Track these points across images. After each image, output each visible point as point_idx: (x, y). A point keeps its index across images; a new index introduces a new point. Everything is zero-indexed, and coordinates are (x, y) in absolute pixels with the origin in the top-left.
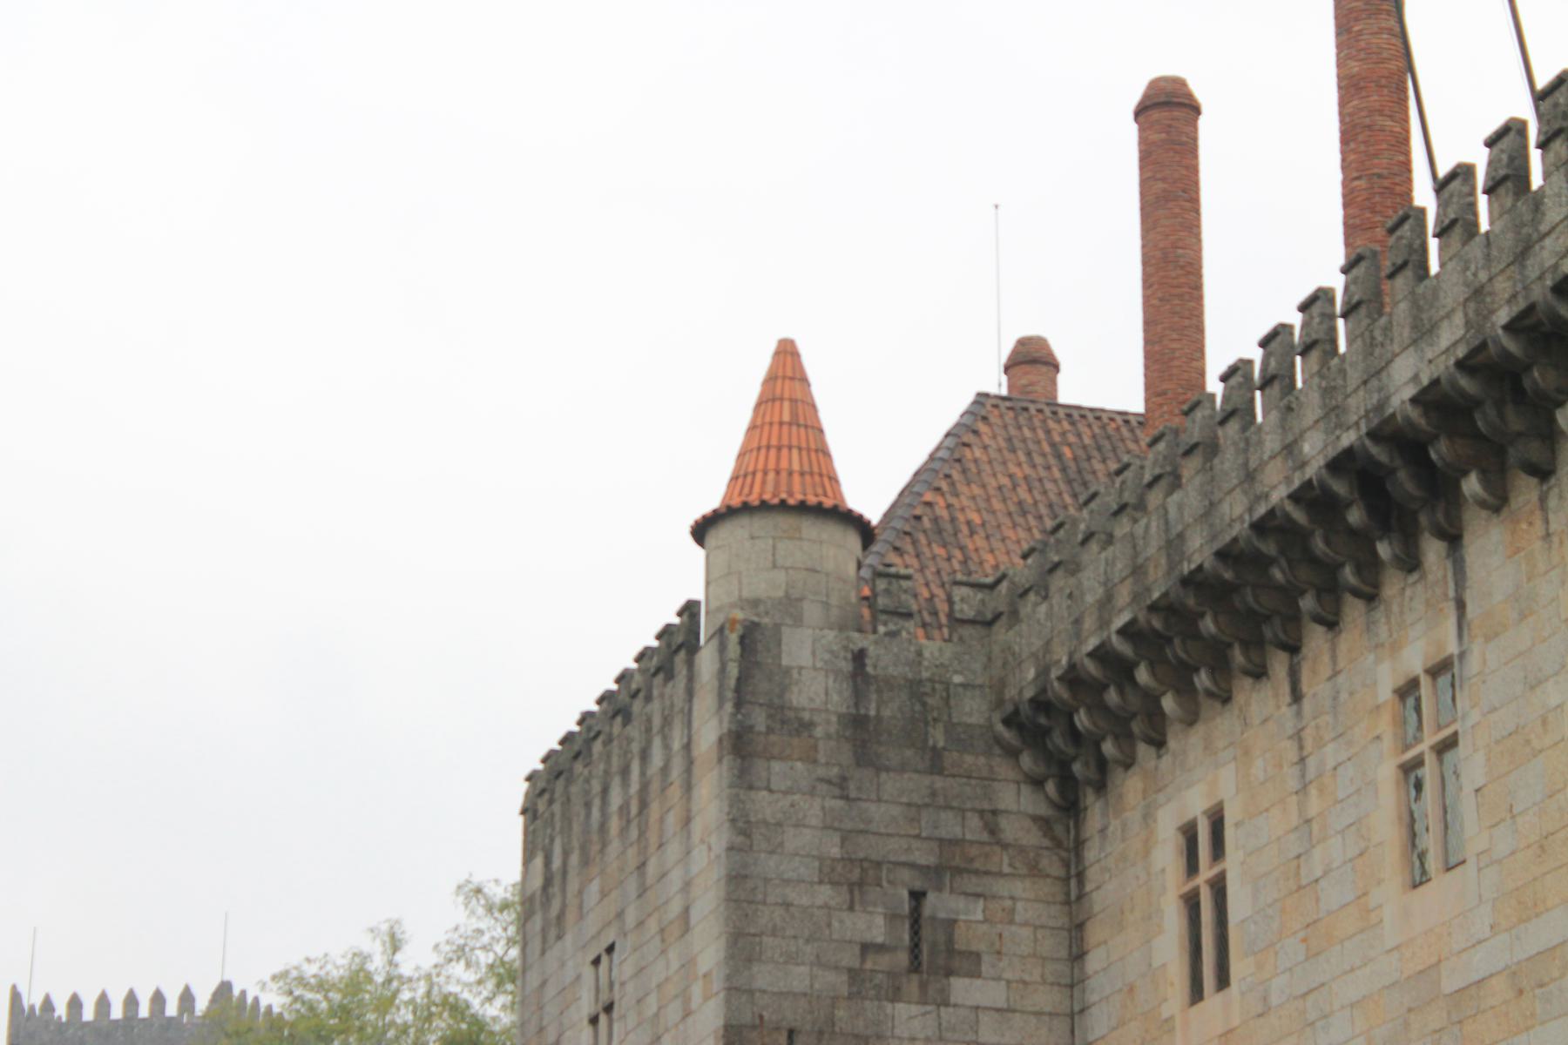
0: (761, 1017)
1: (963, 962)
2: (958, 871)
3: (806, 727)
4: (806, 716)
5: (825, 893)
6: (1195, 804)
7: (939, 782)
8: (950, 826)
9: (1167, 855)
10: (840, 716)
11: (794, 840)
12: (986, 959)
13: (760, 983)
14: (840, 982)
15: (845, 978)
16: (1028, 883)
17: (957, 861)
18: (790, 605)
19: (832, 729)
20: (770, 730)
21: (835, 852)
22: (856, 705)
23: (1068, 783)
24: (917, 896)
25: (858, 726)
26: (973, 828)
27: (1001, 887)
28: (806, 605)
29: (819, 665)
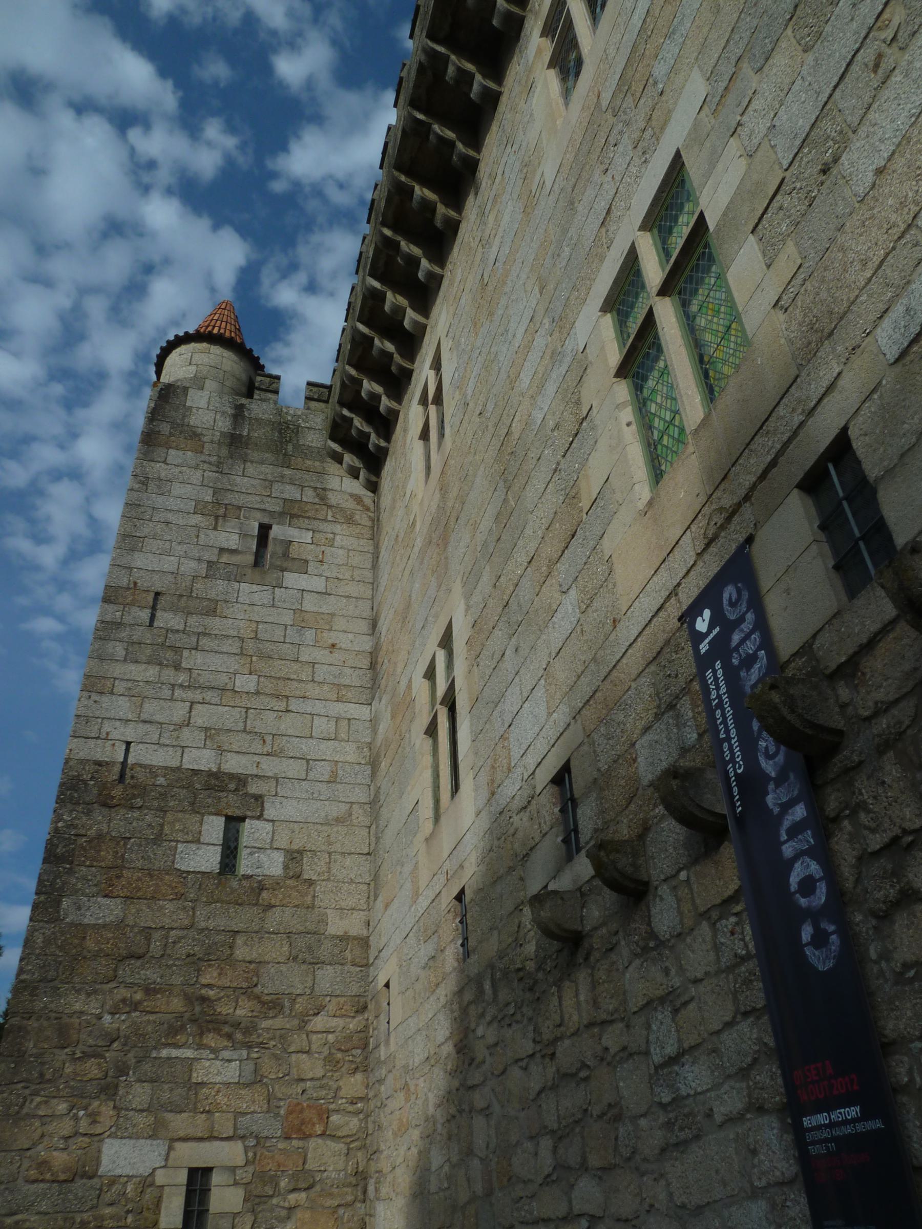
0: (135, 583)
1: (289, 560)
2: (293, 516)
4: (199, 431)
5: (197, 519)
7: (287, 472)
8: (292, 492)
10: (222, 433)
12: (311, 564)
13: (139, 564)
15: (204, 565)
16: (345, 526)
17: (295, 511)
19: (216, 439)
20: (171, 435)
21: (209, 498)
22: (234, 429)
24: (264, 529)
25: (235, 443)
26: (309, 495)
27: (327, 527)
28: (207, 381)
29: (211, 408)
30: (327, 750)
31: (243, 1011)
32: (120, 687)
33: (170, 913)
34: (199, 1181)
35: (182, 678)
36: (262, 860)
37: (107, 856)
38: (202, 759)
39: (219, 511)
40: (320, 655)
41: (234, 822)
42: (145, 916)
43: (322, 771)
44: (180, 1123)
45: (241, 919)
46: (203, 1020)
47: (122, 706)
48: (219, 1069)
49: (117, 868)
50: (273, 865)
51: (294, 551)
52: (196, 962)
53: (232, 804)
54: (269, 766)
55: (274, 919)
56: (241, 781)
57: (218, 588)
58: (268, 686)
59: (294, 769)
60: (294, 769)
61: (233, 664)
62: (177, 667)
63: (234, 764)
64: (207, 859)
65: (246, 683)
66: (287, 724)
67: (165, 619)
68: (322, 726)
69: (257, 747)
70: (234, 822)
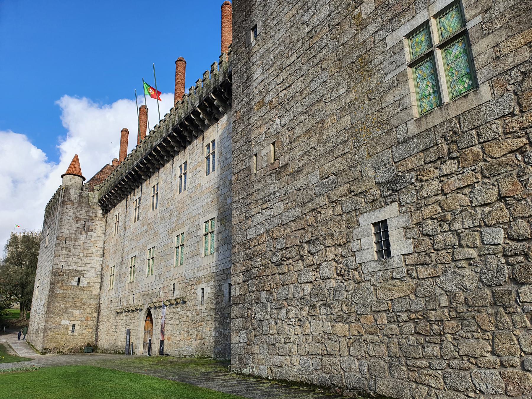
14: (74, 232)
27: (96, 222)
31: (80, 305)
32: (61, 256)
35: (71, 253)
36: (83, 284)
38: (75, 268)
40: (94, 248)
41: (79, 279)
43: (93, 269)
50: (85, 284)
53: (79, 275)
54: (85, 269)
56: (81, 271)
58: (85, 255)
59: (89, 269)
62: (70, 252)
63: (79, 268)
64: (76, 283)
65: (81, 254)
66: (88, 261)
68: (94, 262)
69: (83, 265)
70: (79, 279)
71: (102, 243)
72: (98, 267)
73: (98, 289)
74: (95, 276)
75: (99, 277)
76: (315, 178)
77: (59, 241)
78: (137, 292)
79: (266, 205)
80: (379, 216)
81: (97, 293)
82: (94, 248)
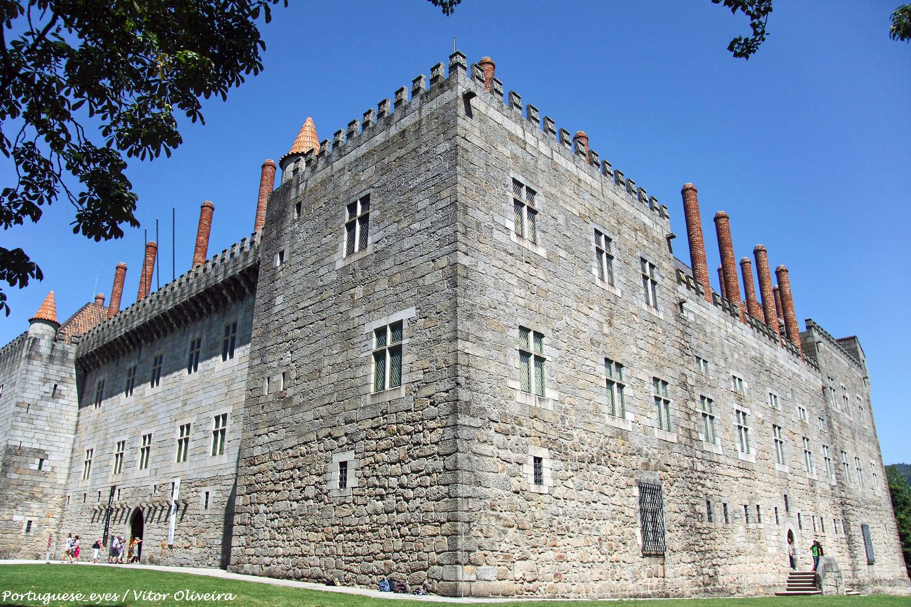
1: (61, 396)
3: (41, 356)
6: (101, 378)
8: (63, 375)
9: (96, 385)
11: (35, 373)
18: (43, 335)
23: (85, 372)
24: (56, 386)
25: (51, 358)
26: (68, 376)
30: (63, 445)
31: (40, 496)
33: (27, 477)
34: (30, 522)
36: (46, 467)
37: (16, 465)
38: (37, 446)
39: (45, 380)
40: (64, 422)
41: (42, 460)
42: (23, 477)
44: (27, 514)
45: (41, 479)
46: (32, 497)
47: (19, 433)
48: (34, 505)
49: (18, 468)
50: (49, 469)
51: (62, 393)
52: (32, 486)
54: (50, 448)
55: (47, 480)
56: (44, 451)
57: (43, 403)
60: (55, 449)
61: (45, 423)
63: (43, 447)
64: (36, 467)
65: (47, 428)
66: (56, 439)
67: (31, 411)
68: (63, 439)
70: (42, 460)
71: (76, 414)
72: (68, 446)
73: (65, 476)
74: (63, 458)
75: (68, 460)
76: (309, 416)
77: (18, 409)
78: (123, 486)
79: (272, 429)
80: (342, 457)
81: (63, 482)
82: (64, 422)
